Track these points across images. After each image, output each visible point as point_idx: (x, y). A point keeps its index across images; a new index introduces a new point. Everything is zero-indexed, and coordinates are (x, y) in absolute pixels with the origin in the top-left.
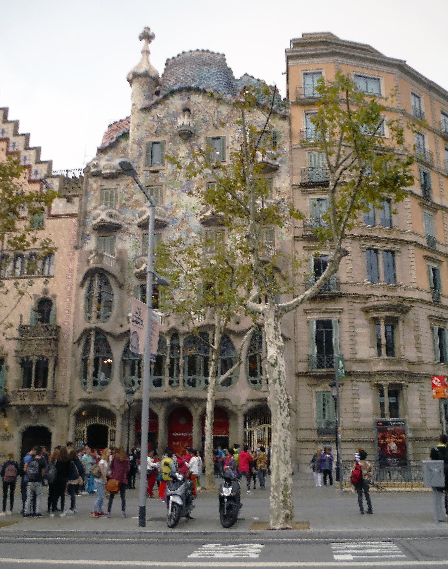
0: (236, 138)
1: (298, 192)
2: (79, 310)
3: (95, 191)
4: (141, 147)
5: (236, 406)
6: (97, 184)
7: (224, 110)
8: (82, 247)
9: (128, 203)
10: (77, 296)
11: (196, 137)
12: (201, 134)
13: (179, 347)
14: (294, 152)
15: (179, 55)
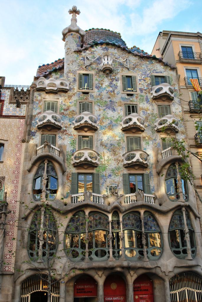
0: (142, 78)
1: (187, 116)
2: (26, 190)
3: (40, 101)
4: (75, 76)
5: (164, 272)
6: (42, 97)
7: (133, 59)
8: (28, 142)
9: (66, 113)
10: (24, 178)
11: (114, 74)
12: (118, 72)
13: (118, 223)
14: (182, 90)
15: (90, 30)
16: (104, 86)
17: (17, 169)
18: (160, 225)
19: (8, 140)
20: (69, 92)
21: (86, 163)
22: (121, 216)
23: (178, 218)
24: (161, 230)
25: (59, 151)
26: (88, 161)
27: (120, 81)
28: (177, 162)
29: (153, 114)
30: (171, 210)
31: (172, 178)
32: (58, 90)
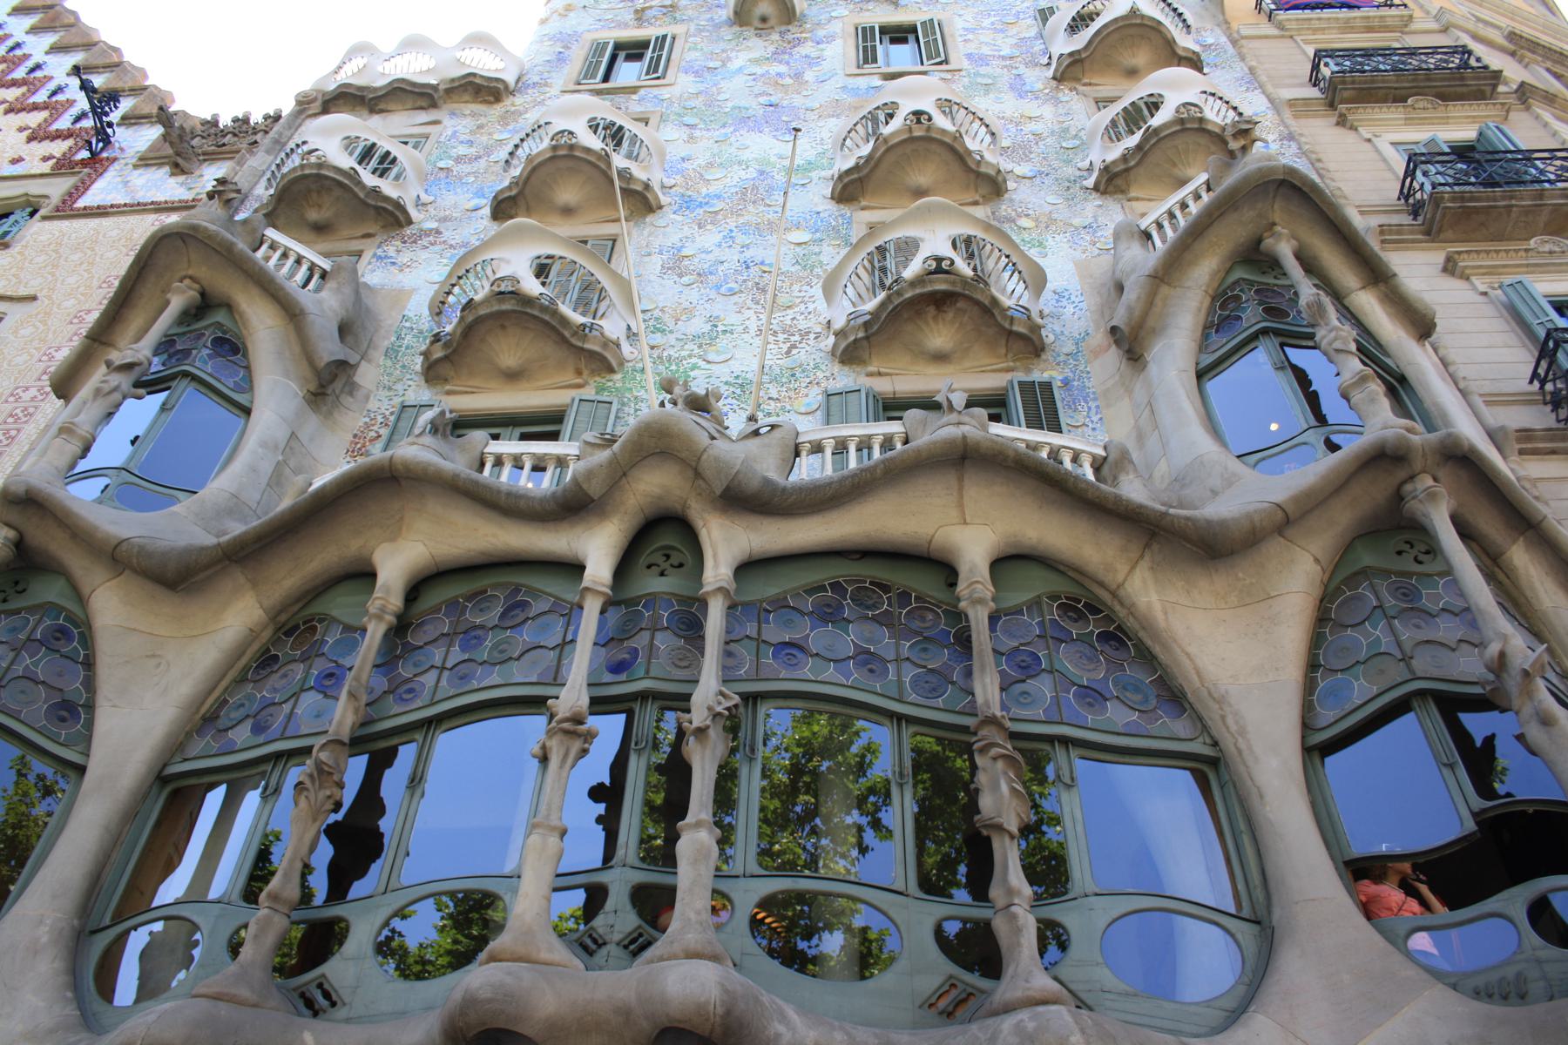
16: (735, 65)
17: (10, 420)
18: (1190, 683)
19: (34, 298)
20: (508, 101)
21: (506, 307)
22: (725, 544)
23: (1390, 602)
24: (1215, 744)
25: (324, 275)
26: (528, 301)
27: (839, 42)
28: (1278, 228)
29: (1066, 130)
30: (1285, 522)
31: (1254, 337)
32: (442, 87)
